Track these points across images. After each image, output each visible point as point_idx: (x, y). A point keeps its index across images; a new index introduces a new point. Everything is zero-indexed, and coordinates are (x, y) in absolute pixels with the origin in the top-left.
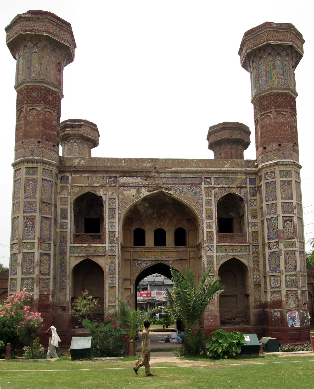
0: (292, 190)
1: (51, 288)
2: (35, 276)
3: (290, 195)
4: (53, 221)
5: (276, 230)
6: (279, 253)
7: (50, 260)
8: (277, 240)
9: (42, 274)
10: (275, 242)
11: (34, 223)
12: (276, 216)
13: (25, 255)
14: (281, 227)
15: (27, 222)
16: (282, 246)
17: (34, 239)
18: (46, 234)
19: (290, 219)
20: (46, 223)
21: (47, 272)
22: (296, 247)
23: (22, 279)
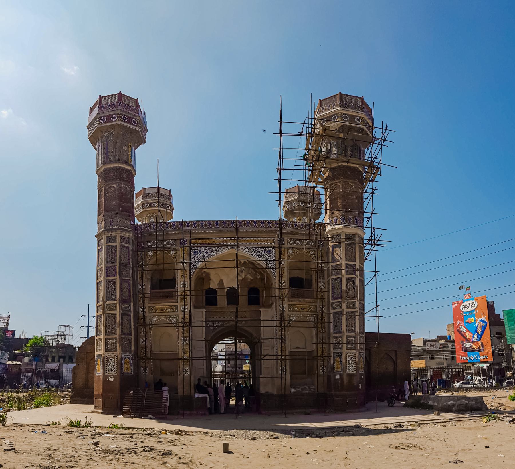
0: (355, 253)
2: (117, 336)
3: (353, 258)
5: (339, 290)
6: (341, 314)
7: (131, 320)
8: (340, 300)
9: (124, 334)
10: (338, 302)
12: (340, 276)
13: (108, 317)
14: (344, 288)
15: (109, 285)
16: (344, 306)
18: (126, 294)
19: (353, 280)
20: (125, 284)
21: (129, 332)
22: (356, 308)
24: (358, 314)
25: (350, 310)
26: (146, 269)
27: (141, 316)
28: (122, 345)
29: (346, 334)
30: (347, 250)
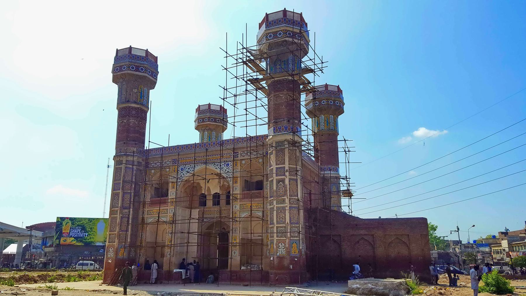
1: (129, 240)
2: (116, 232)
4: (133, 194)
9: (122, 231)
11: (118, 197)
17: (118, 207)
23: (110, 234)
24: (287, 208)
25: (282, 205)
26: (148, 183)
27: (140, 217)
28: (119, 239)
29: (276, 225)
30: (277, 156)
